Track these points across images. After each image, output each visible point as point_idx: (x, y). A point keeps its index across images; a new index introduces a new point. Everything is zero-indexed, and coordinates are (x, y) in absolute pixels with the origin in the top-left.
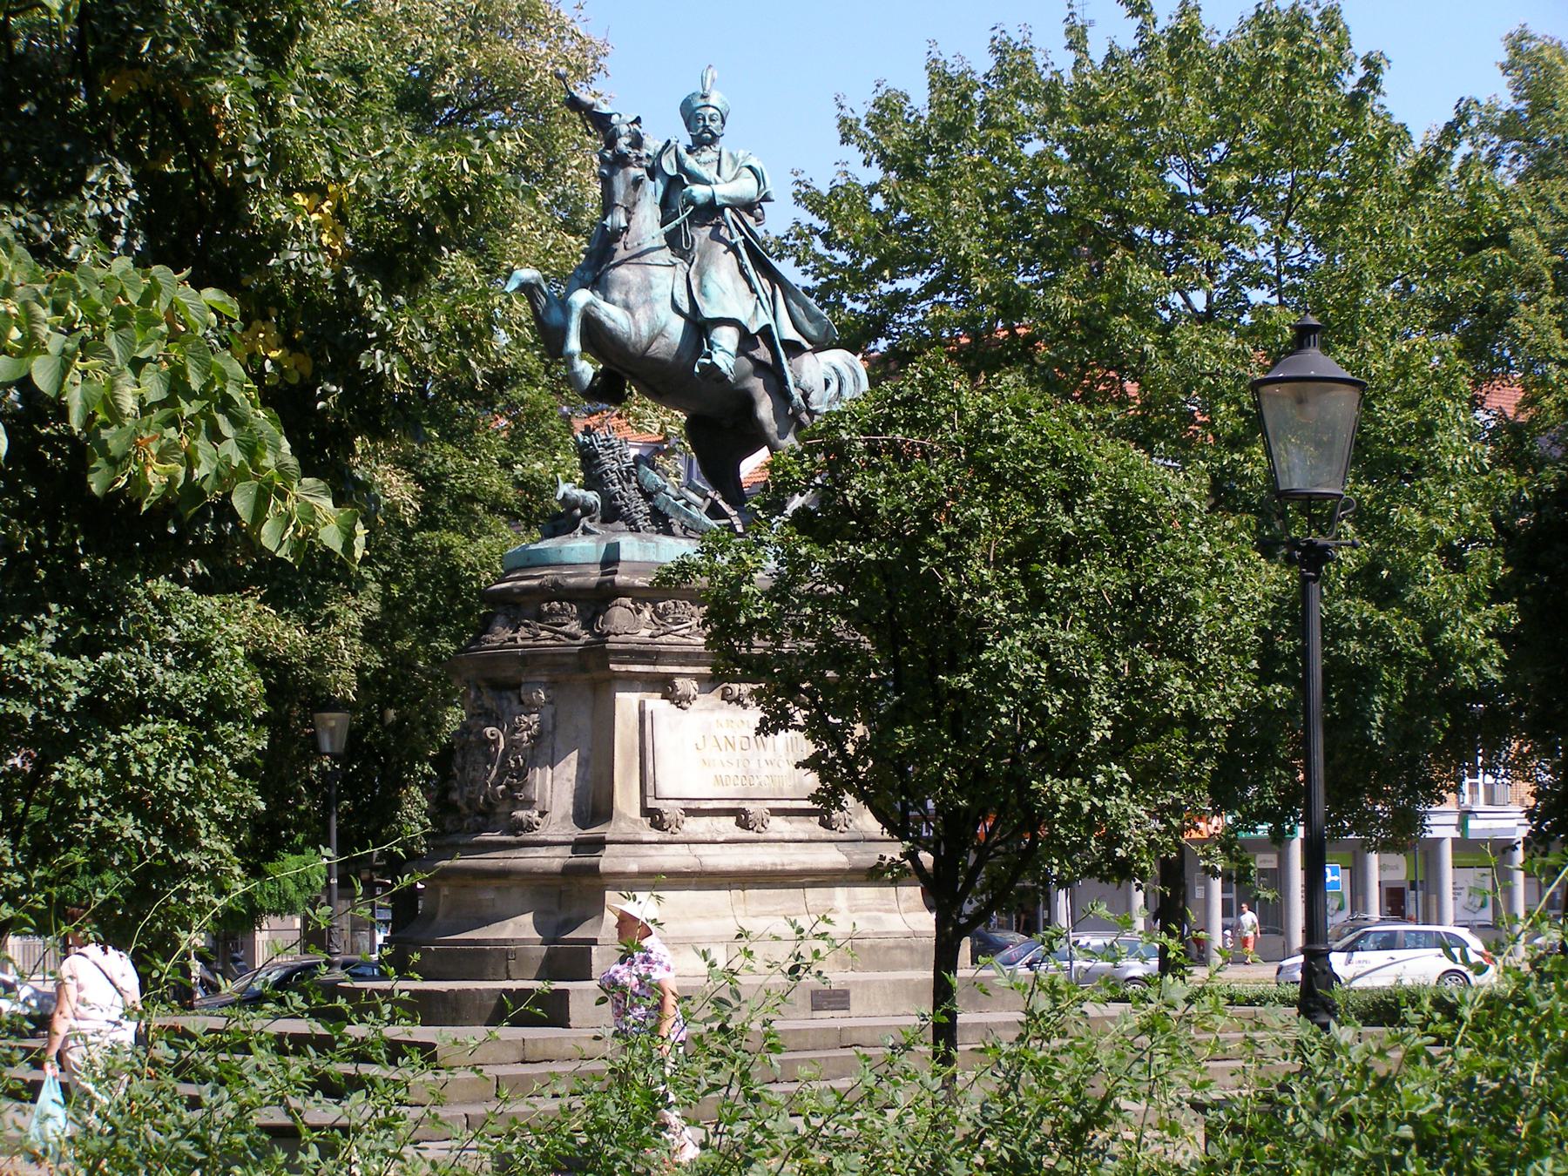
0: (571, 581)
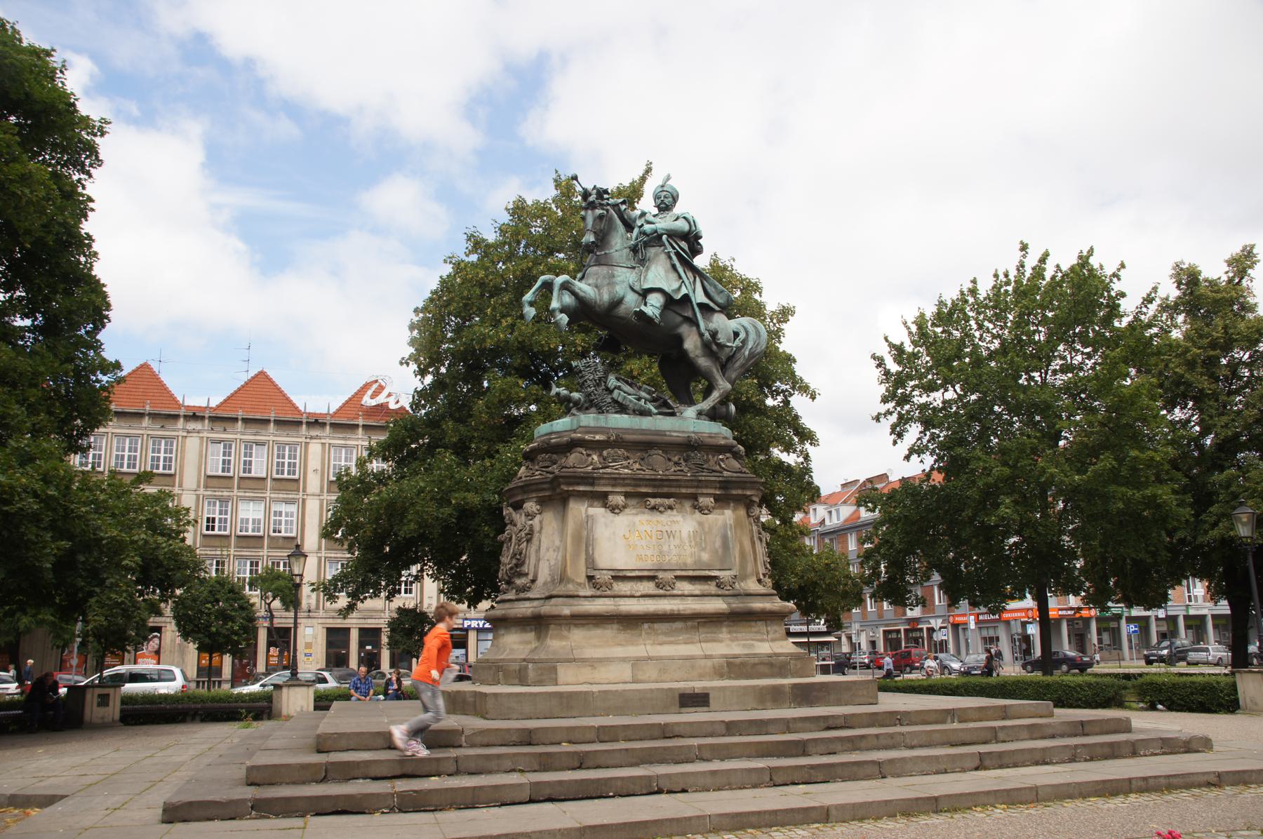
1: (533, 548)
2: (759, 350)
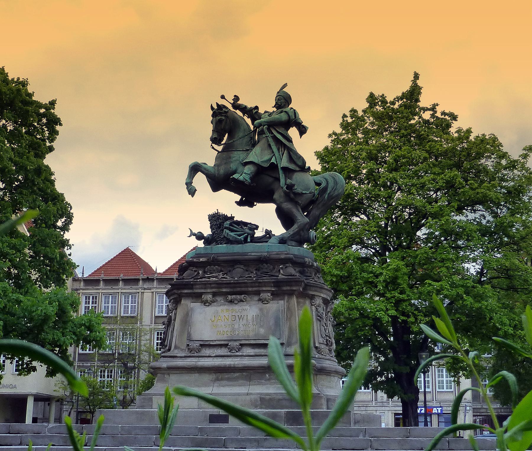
2: (336, 193)
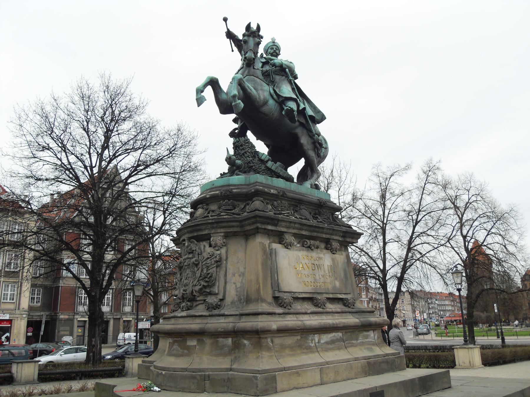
0: (235, 190)
1: (222, 273)
